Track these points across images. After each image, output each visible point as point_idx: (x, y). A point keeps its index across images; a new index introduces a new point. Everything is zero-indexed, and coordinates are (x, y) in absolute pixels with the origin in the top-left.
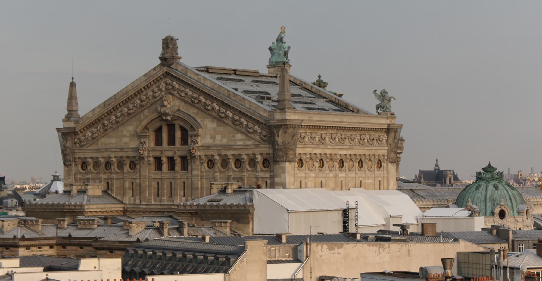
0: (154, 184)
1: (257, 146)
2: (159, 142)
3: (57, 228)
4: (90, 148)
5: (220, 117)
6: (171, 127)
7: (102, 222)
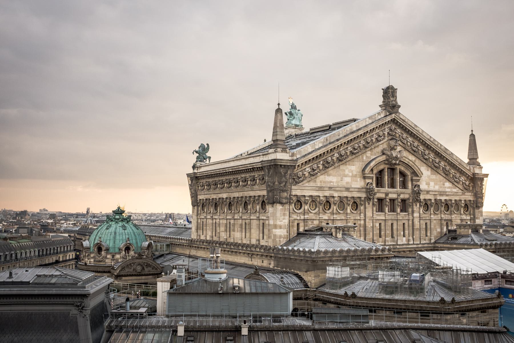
0: (378, 225)
1: (463, 194)
2: (379, 183)
4: (307, 185)
5: (435, 166)
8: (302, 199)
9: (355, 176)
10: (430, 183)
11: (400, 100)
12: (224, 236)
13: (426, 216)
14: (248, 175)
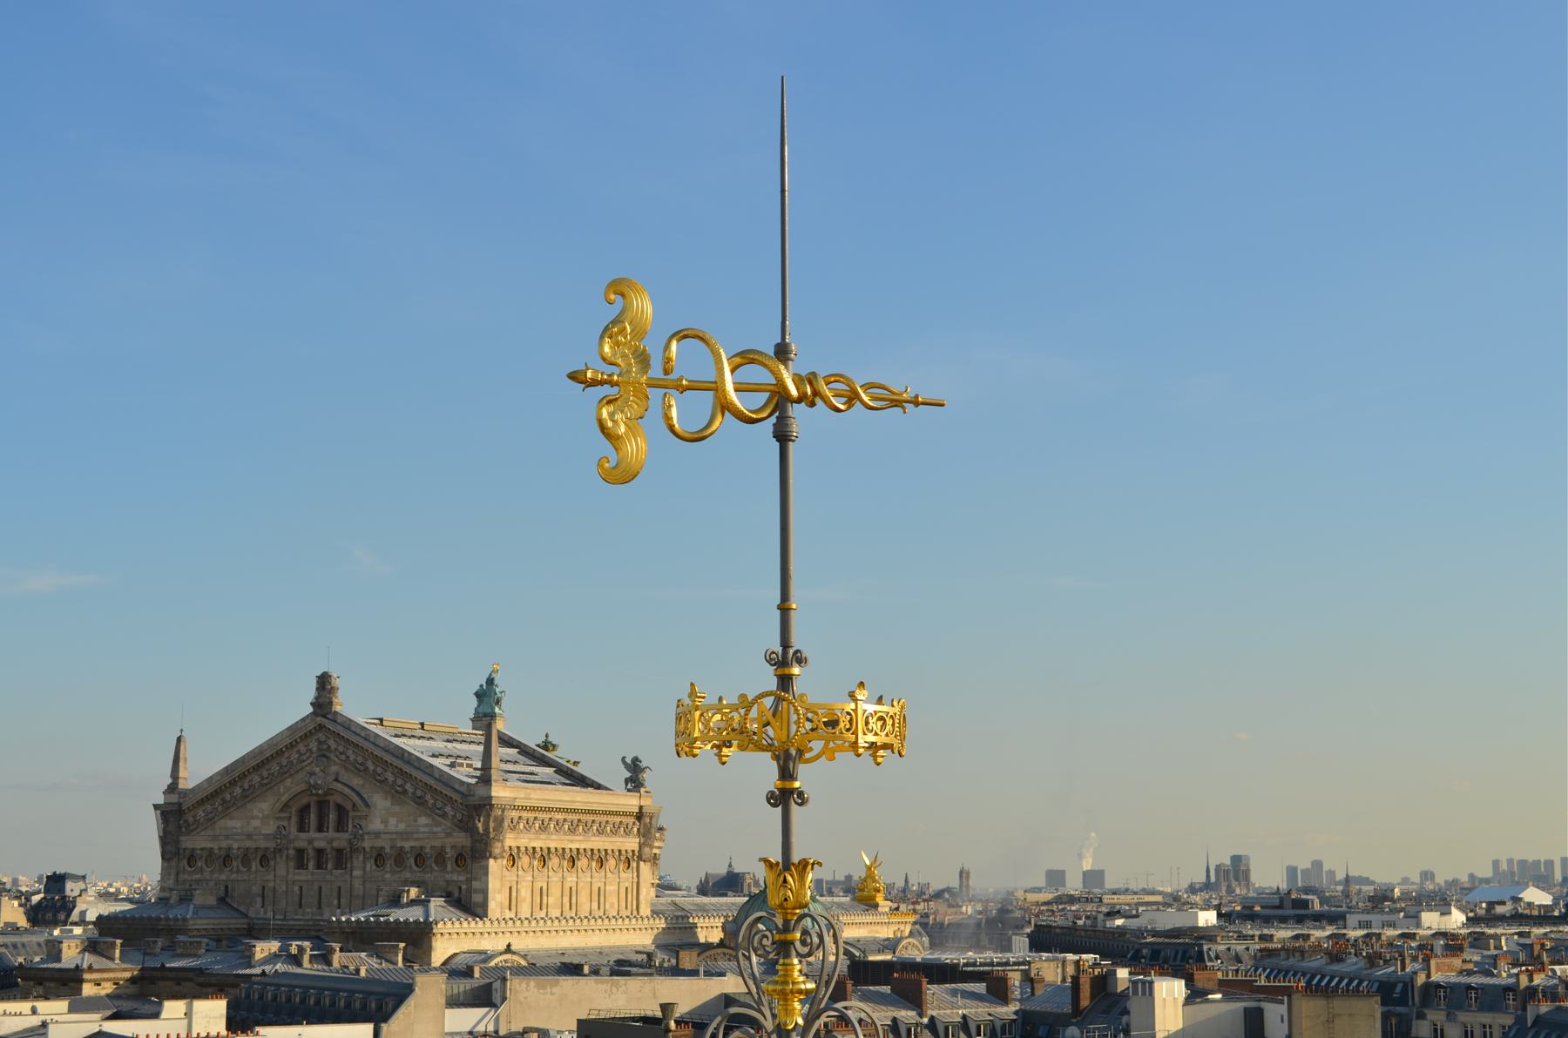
0: (296, 888)
1: (448, 835)
2: (302, 828)
3: (145, 954)
7: (213, 944)
9: (267, 817)
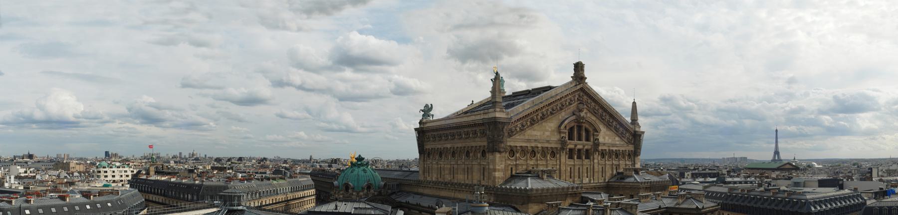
2: (571, 138)
6: (580, 128)
8: (515, 149)
10: (606, 138)
11: (586, 74)
12: (448, 178)
13: (602, 162)
14: (469, 130)
